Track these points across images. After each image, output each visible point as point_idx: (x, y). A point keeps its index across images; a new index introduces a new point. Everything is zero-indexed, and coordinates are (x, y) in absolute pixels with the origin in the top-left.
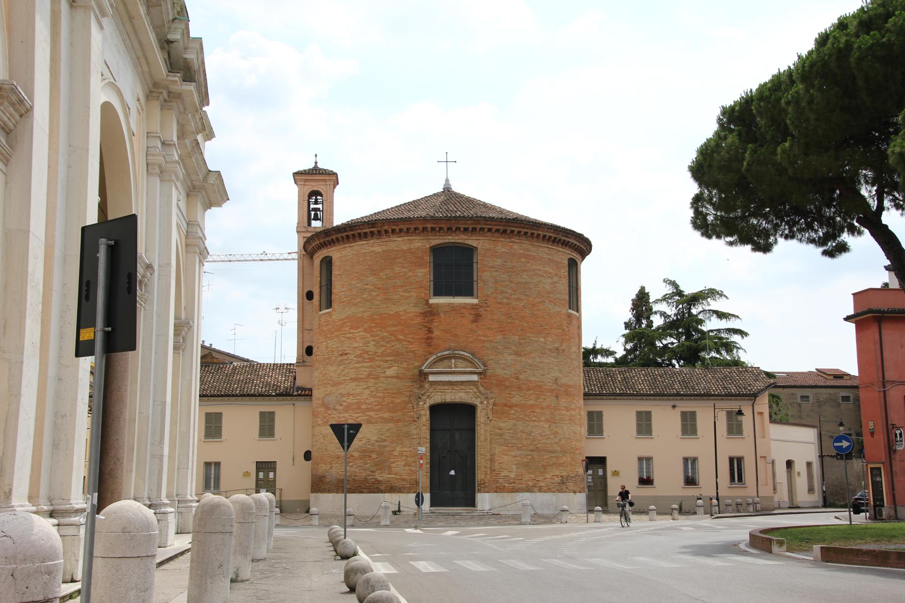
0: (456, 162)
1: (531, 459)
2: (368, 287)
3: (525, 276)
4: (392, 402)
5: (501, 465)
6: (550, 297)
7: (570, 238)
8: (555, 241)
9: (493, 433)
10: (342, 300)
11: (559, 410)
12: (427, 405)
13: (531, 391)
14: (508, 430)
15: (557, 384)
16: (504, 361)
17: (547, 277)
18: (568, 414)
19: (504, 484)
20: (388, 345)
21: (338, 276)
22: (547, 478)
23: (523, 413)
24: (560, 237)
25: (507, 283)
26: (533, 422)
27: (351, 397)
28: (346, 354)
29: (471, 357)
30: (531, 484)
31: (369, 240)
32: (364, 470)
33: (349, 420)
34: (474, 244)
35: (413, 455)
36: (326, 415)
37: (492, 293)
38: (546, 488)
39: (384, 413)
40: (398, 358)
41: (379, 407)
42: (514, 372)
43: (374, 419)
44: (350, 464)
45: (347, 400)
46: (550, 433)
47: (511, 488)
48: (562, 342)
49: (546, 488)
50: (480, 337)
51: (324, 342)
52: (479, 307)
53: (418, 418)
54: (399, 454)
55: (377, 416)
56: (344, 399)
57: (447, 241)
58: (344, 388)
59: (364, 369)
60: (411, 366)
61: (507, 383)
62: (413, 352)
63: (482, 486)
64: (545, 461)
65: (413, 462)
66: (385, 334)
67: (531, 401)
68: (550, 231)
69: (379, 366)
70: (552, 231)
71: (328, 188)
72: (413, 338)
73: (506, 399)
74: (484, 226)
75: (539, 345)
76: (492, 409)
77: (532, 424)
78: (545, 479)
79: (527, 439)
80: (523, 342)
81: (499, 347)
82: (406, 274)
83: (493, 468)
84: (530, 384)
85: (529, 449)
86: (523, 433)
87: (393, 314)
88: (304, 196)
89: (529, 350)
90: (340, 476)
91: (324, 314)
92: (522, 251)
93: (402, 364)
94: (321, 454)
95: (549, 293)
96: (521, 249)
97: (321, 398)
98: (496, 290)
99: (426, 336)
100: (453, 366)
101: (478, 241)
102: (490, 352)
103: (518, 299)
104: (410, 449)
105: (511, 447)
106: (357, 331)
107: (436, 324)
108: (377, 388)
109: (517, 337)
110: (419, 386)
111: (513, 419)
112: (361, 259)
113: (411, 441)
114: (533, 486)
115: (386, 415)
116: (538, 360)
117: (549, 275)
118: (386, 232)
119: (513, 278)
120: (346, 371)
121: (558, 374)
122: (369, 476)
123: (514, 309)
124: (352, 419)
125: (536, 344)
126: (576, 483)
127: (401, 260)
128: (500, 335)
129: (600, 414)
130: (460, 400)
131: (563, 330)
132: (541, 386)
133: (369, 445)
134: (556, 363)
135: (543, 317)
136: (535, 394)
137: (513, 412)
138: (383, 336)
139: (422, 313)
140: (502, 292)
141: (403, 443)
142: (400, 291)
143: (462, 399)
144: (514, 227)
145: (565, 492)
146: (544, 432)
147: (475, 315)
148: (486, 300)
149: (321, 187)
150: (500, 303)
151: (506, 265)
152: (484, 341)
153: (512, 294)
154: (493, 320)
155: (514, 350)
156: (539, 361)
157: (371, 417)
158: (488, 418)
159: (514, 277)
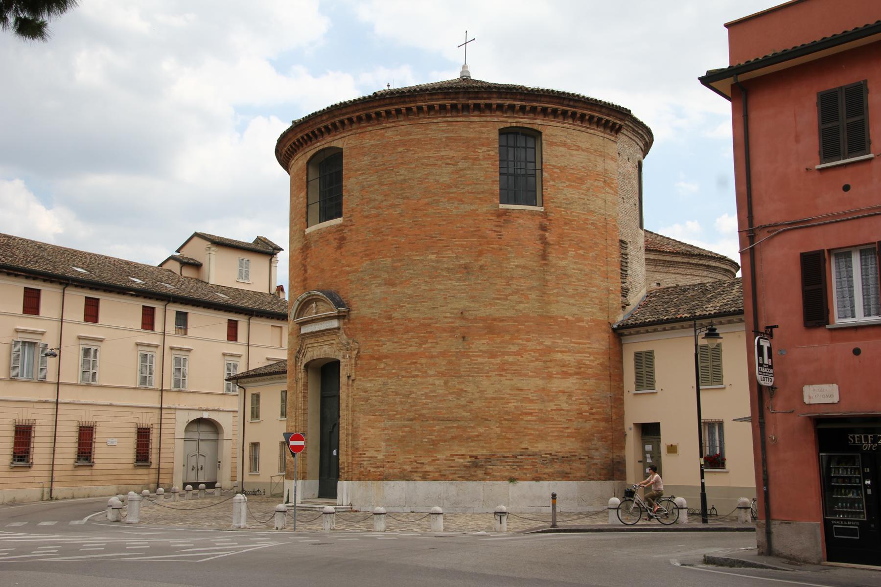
0: (474, 39)
5: (366, 441)
7: (489, 98)
9: (357, 397)
11: (468, 357)
12: (303, 366)
14: (376, 392)
16: (371, 296)
17: (444, 165)
19: (368, 469)
22: (438, 460)
23: (396, 367)
25: (376, 187)
30: (408, 468)
34: (337, 144)
37: (357, 205)
42: (384, 309)
47: (379, 473)
49: (437, 475)
52: (343, 228)
61: (375, 327)
64: (436, 434)
67: (410, 348)
70: (440, 96)
73: (373, 349)
76: (356, 364)
77: (411, 380)
78: (433, 460)
79: (402, 403)
80: (399, 264)
81: (367, 278)
83: (356, 446)
85: (406, 417)
86: (397, 394)
89: (408, 275)
92: (399, 137)
95: (449, 186)
96: (397, 135)
98: (362, 199)
102: (354, 286)
103: (393, 206)
105: (379, 415)
109: (389, 260)
114: (411, 472)
116: (423, 287)
117: (449, 161)
119: (385, 179)
121: (465, 303)
123: (385, 221)
125: (421, 265)
128: (366, 260)
129: (650, 355)
130: (324, 356)
132: (429, 325)
134: (464, 287)
136: (418, 337)
137: (382, 366)
140: (371, 200)
144: (377, 107)
145: (484, 480)
146: (435, 391)
147: (339, 239)
150: (367, 217)
151: (375, 162)
152: (348, 273)
153: (382, 201)
154: (359, 241)
155: (385, 279)
156: (426, 288)
159: (386, 176)
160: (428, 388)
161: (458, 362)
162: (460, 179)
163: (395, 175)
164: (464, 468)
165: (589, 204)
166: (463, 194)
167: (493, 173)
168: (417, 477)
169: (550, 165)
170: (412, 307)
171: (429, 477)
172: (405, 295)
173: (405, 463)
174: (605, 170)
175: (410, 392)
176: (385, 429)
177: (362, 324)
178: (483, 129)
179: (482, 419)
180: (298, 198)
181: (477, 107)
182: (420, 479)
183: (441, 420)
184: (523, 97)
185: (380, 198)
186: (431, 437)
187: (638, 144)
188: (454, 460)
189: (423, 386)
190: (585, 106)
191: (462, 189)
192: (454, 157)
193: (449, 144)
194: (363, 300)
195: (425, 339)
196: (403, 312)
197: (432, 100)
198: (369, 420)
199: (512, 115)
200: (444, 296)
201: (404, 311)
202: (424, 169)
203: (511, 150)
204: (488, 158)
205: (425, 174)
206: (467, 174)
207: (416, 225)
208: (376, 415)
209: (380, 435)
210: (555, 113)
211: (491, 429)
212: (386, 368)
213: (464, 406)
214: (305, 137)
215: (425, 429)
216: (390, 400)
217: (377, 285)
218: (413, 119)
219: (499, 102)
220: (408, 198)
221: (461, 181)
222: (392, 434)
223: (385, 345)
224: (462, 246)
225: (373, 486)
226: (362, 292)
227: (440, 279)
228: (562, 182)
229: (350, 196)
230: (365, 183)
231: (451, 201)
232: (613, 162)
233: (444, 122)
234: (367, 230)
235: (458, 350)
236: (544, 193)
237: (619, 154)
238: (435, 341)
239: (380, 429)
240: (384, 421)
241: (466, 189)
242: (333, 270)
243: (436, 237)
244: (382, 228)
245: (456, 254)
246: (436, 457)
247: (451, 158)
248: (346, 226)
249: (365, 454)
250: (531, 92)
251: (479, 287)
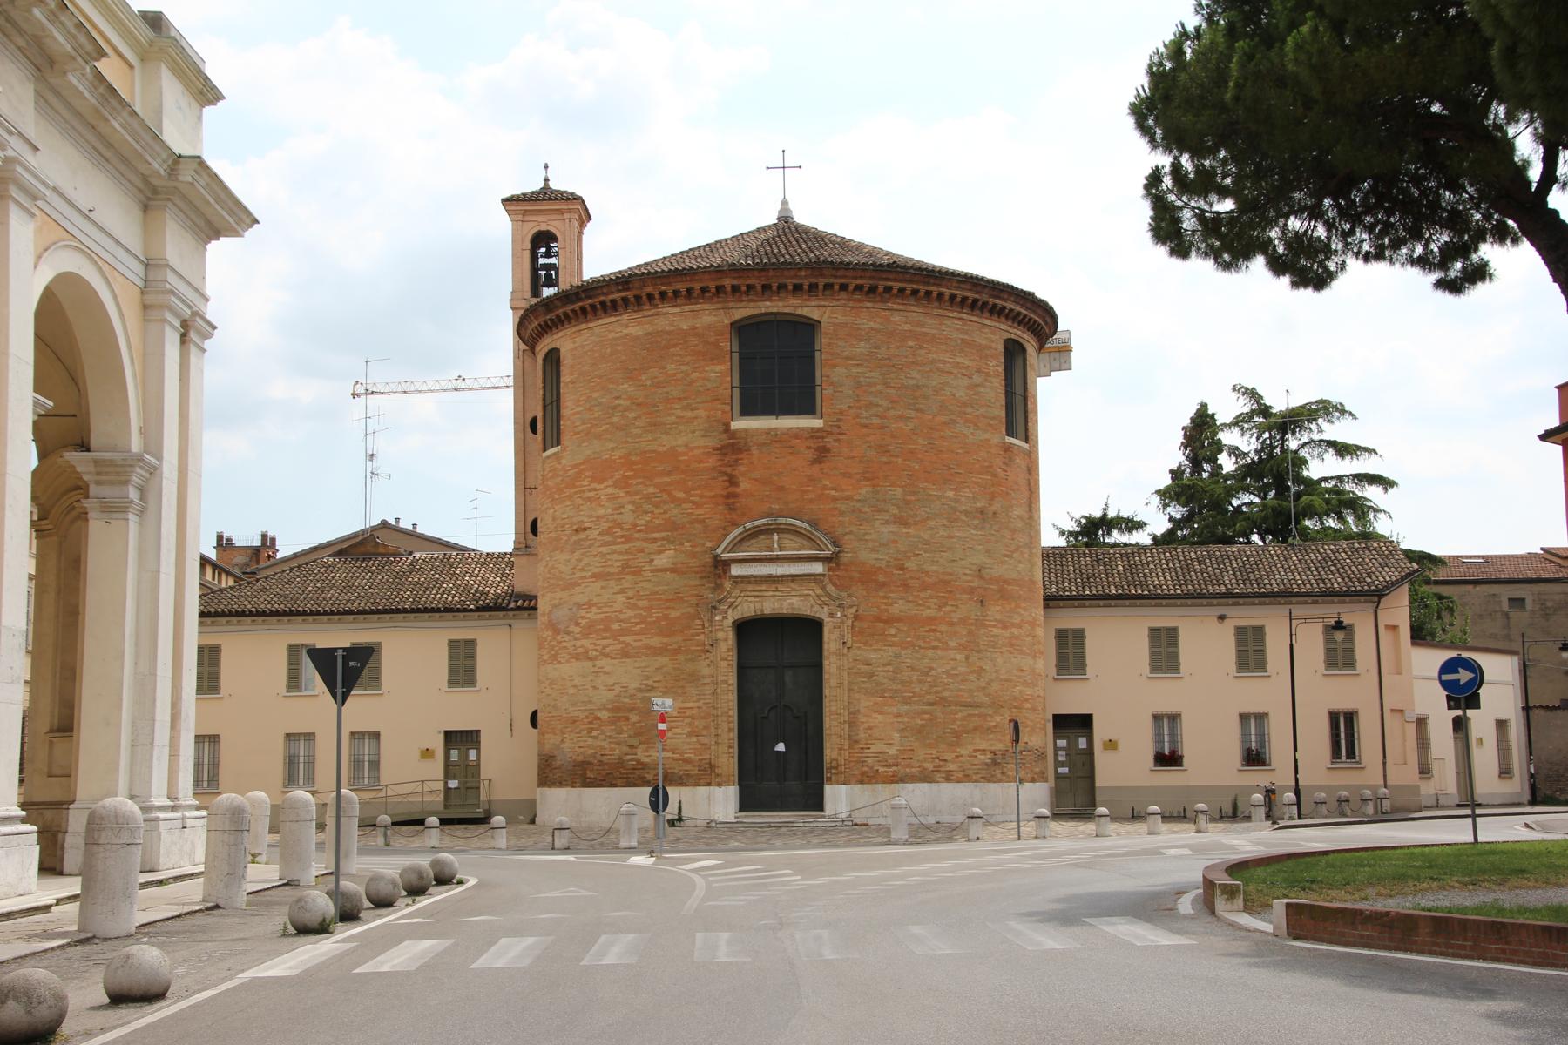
0: (800, 167)
1: (931, 720)
2: (621, 402)
3: (914, 374)
4: (666, 617)
5: (869, 732)
6: (965, 413)
7: (1006, 300)
8: (975, 306)
9: (854, 671)
10: (576, 430)
11: (986, 626)
12: (730, 621)
13: (929, 592)
14: (884, 665)
15: (981, 577)
16: (874, 536)
17: (959, 376)
18: (1007, 633)
19: (876, 768)
20: (657, 511)
21: (570, 385)
22: (962, 756)
24: (985, 297)
25: (879, 387)
26: (933, 651)
27: (594, 610)
28: (585, 529)
29: (809, 528)
30: (929, 766)
31: (620, 315)
32: (618, 744)
33: (590, 652)
34: (814, 314)
35: (702, 714)
36: (554, 643)
37: (849, 407)
38: (960, 775)
39: (652, 638)
40: (675, 533)
41: (643, 626)
42: (895, 556)
43: (634, 648)
44: (594, 733)
45: (588, 615)
46: (968, 670)
47: (891, 774)
48: (992, 498)
49: (960, 775)
50: (828, 492)
51: (550, 508)
52: (825, 435)
53: (712, 645)
54: (679, 713)
55: (639, 644)
56: (583, 613)
57: (763, 310)
58: (582, 593)
59: (615, 556)
60: (697, 550)
61: (881, 578)
62: (702, 521)
63: (833, 771)
64: (959, 723)
65: (705, 728)
66: (651, 490)
67: (929, 611)
68: (962, 286)
69: (642, 551)
70: (968, 286)
71: (567, 225)
72: (701, 496)
73: (878, 608)
74: (832, 280)
75: (943, 504)
76: (853, 626)
77: (930, 653)
78: (957, 757)
79: (920, 681)
80: (913, 498)
81: (866, 509)
82: (688, 375)
83: (854, 738)
84: (926, 579)
85: (925, 701)
86: (913, 669)
87: (665, 452)
88: (523, 241)
89: (923, 513)
90: (578, 755)
91: (548, 457)
92: (907, 327)
93: (682, 544)
94: (547, 715)
95: (965, 405)
97: (547, 611)
98: (858, 401)
99: (724, 493)
100: (776, 546)
101: (823, 309)
102: (847, 519)
103: (901, 418)
104: (700, 704)
105: (891, 697)
106: (602, 486)
107: (743, 469)
108: (638, 592)
109: (900, 490)
110: (713, 585)
112: (609, 350)
113: (700, 688)
114: (933, 771)
115: (655, 641)
117: (964, 371)
118: (650, 297)
120: (586, 561)
122: (627, 754)
123: (893, 436)
124: (596, 650)
125: (938, 502)
126: (1024, 764)
127: (678, 349)
128: (866, 486)
129: (1079, 635)
130: (790, 611)
131: (995, 475)
132: (949, 582)
133: (625, 697)
135: (952, 452)
137: (893, 631)
138: (648, 494)
139: (718, 449)
140: (870, 405)
141: (685, 693)
142: (677, 409)
143: (793, 609)
144: (890, 280)
145: (1000, 781)
147: (817, 449)
148: (839, 420)
149: (554, 223)
150: (866, 426)
152: (835, 499)
155: (894, 515)
156: (945, 534)
157: (627, 644)
158: (844, 643)
159: (893, 375)
164: (986, 767)
170: (929, 557)
171: (952, 778)
173: (925, 760)
177: (860, 572)
182: (943, 780)
186: (953, 727)
192: (969, 367)
197: (957, 288)
209: (893, 723)
212: (899, 635)
213: (984, 688)
222: (908, 722)
223: (896, 603)
225: (883, 791)
226: (860, 529)
229: (835, 392)
230: (862, 379)
233: (960, 319)
234: (868, 444)
239: (891, 716)
244: (888, 445)
245: (973, 493)
248: (831, 433)
249: (869, 748)
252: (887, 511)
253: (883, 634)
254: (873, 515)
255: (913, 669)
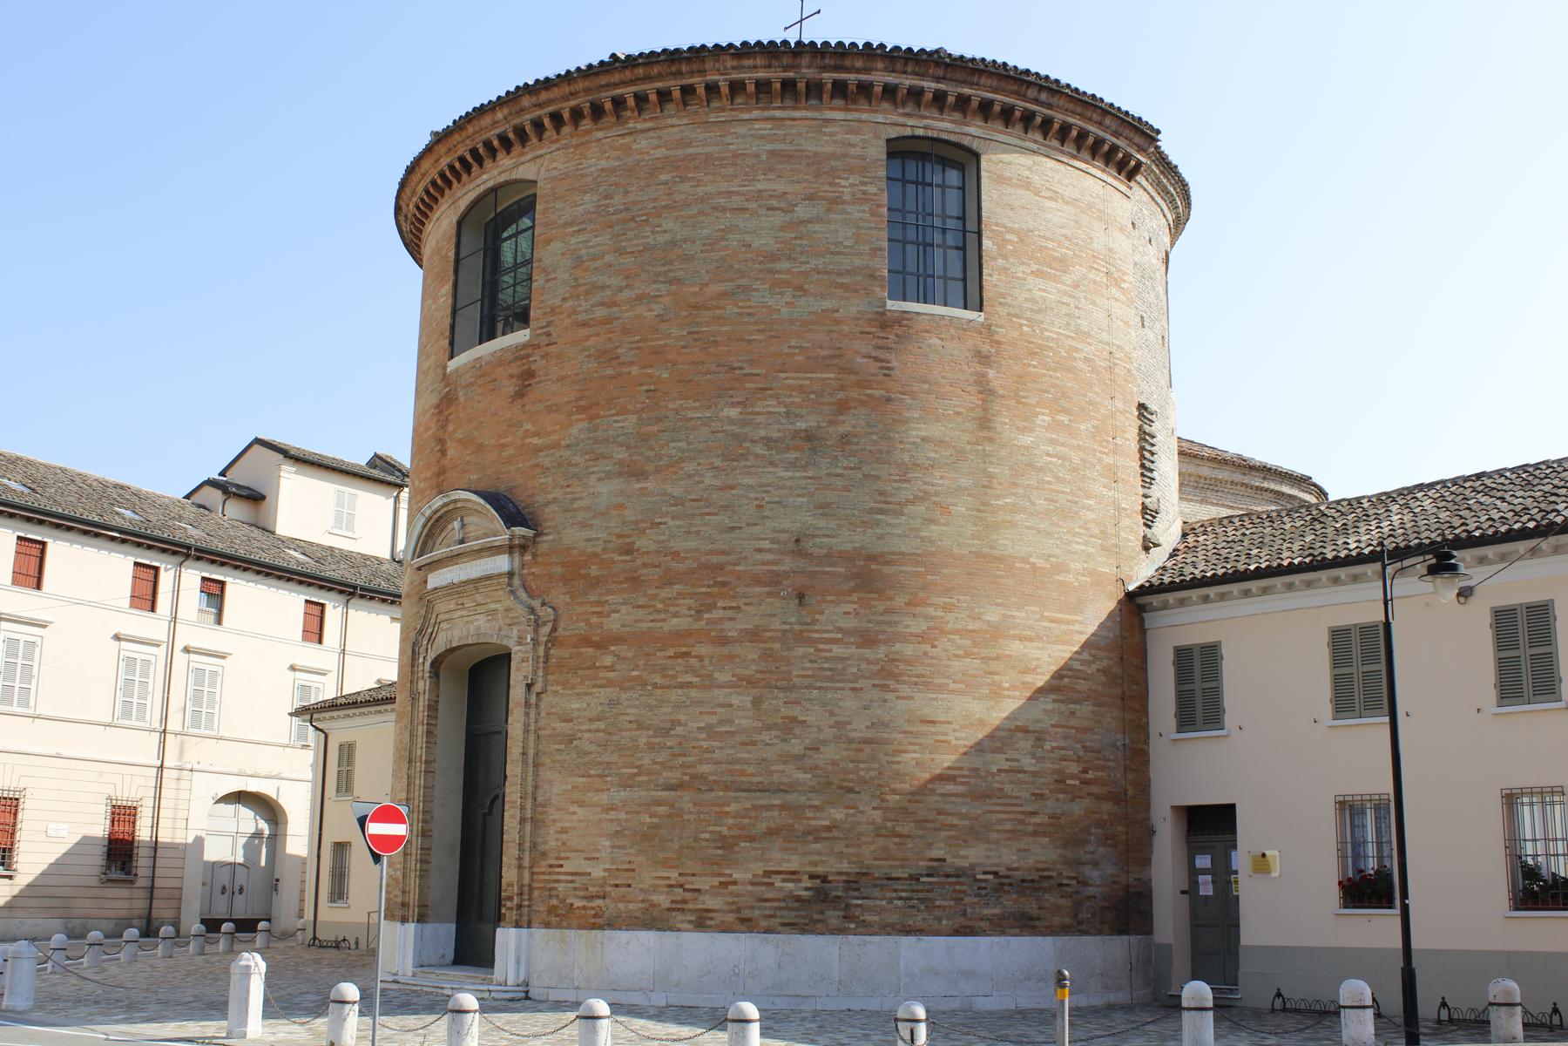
0: (819, 12)
1: (670, 816)
5: (564, 836)
7: (867, 70)
9: (548, 732)
11: (810, 642)
13: (678, 586)
14: (590, 720)
16: (586, 502)
17: (762, 211)
19: (569, 901)
22: (735, 883)
23: (641, 663)
25: (608, 258)
26: (680, 692)
30: (663, 900)
34: (526, 172)
38: (730, 918)
49: (730, 918)
52: (530, 351)
61: (594, 570)
64: (731, 821)
70: (759, 61)
73: (587, 622)
74: (538, 113)
76: (547, 657)
77: (674, 695)
78: (724, 884)
79: (651, 747)
80: (655, 428)
81: (578, 459)
84: (674, 565)
85: (661, 781)
86: (640, 726)
95: (773, 257)
96: (658, 147)
102: (550, 479)
105: (598, 776)
109: (633, 418)
111: (609, 683)
114: (669, 909)
117: (775, 203)
119: (629, 240)
123: (626, 332)
125: (705, 430)
128: (577, 420)
129: (1211, 653)
132: (721, 567)
134: (803, 482)
136: (691, 596)
140: (595, 288)
144: (617, 85)
145: (841, 931)
146: (730, 721)
150: (584, 324)
152: (538, 450)
155: (621, 463)
156: (717, 482)
159: (630, 234)
160: (715, 713)
161: (786, 654)
162: (799, 242)
163: (653, 232)
165: (1079, 318)
166: (806, 274)
167: (874, 232)
168: (682, 922)
169: (997, 224)
170: (680, 526)
172: (667, 498)
173: (655, 889)
174: (1110, 250)
175: (672, 721)
176: (611, 808)
177: (563, 565)
178: (853, 138)
179: (841, 788)
180: (435, 299)
181: (840, 89)
183: (744, 790)
184: (941, 72)
185: (615, 281)
186: (718, 828)
187: (1165, 216)
188: (773, 884)
189: (702, 710)
190: (1071, 106)
191: (802, 263)
192: (785, 193)
193: (776, 166)
194: (567, 511)
195: (710, 601)
196: (662, 538)
197: (740, 68)
198: (575, 787)
199: (917, 112)
200: (755, 503)
201: (664, 534)
202: (717, 218)
203: (911, 188)
204: (865, 198)
205: (722, 230)
206: (815, 232)
207: (696, 340)
208: (590, 776)
209: (600, 821)
210: (1007, 115)
211: (862, 812)
214: (457, 165)
215: (705, 810)
216: (623, 742)
217: (603, 475)
218: (696, 113)
219: (890, 79)
220: (678, 281)
221: (801, 245)
222: (626, 820)
223: (618, 611)
224: (800, 388)
225: (579, 939)
226: (568, 493)
227: (749, 464)
228: (1023, 263)
229: (547, 281)
230: (583, 252)
231: (777, 290)
232: (1124, 237)
233: (767, 119)
234: (585, 353)
235: (787, 627)
236: (984, 283)
237: (1133, 224)
238: (734, 604)
240: (609, 790)
241: (813, 263)
242: (503, 447)
243: (741, 368)
244: (617, 348)
245: (785, 406)
246: (731, 875)
247: (780, 197)
248: (538, 347)
249: (561, 866)
250: (959, 63)
251: (839, 482)
252: (609, 457)
253: (593, 667)
254: (587, 467)
255: (640, 726)
